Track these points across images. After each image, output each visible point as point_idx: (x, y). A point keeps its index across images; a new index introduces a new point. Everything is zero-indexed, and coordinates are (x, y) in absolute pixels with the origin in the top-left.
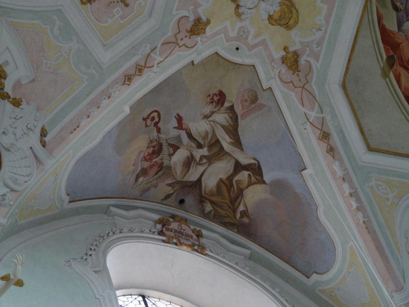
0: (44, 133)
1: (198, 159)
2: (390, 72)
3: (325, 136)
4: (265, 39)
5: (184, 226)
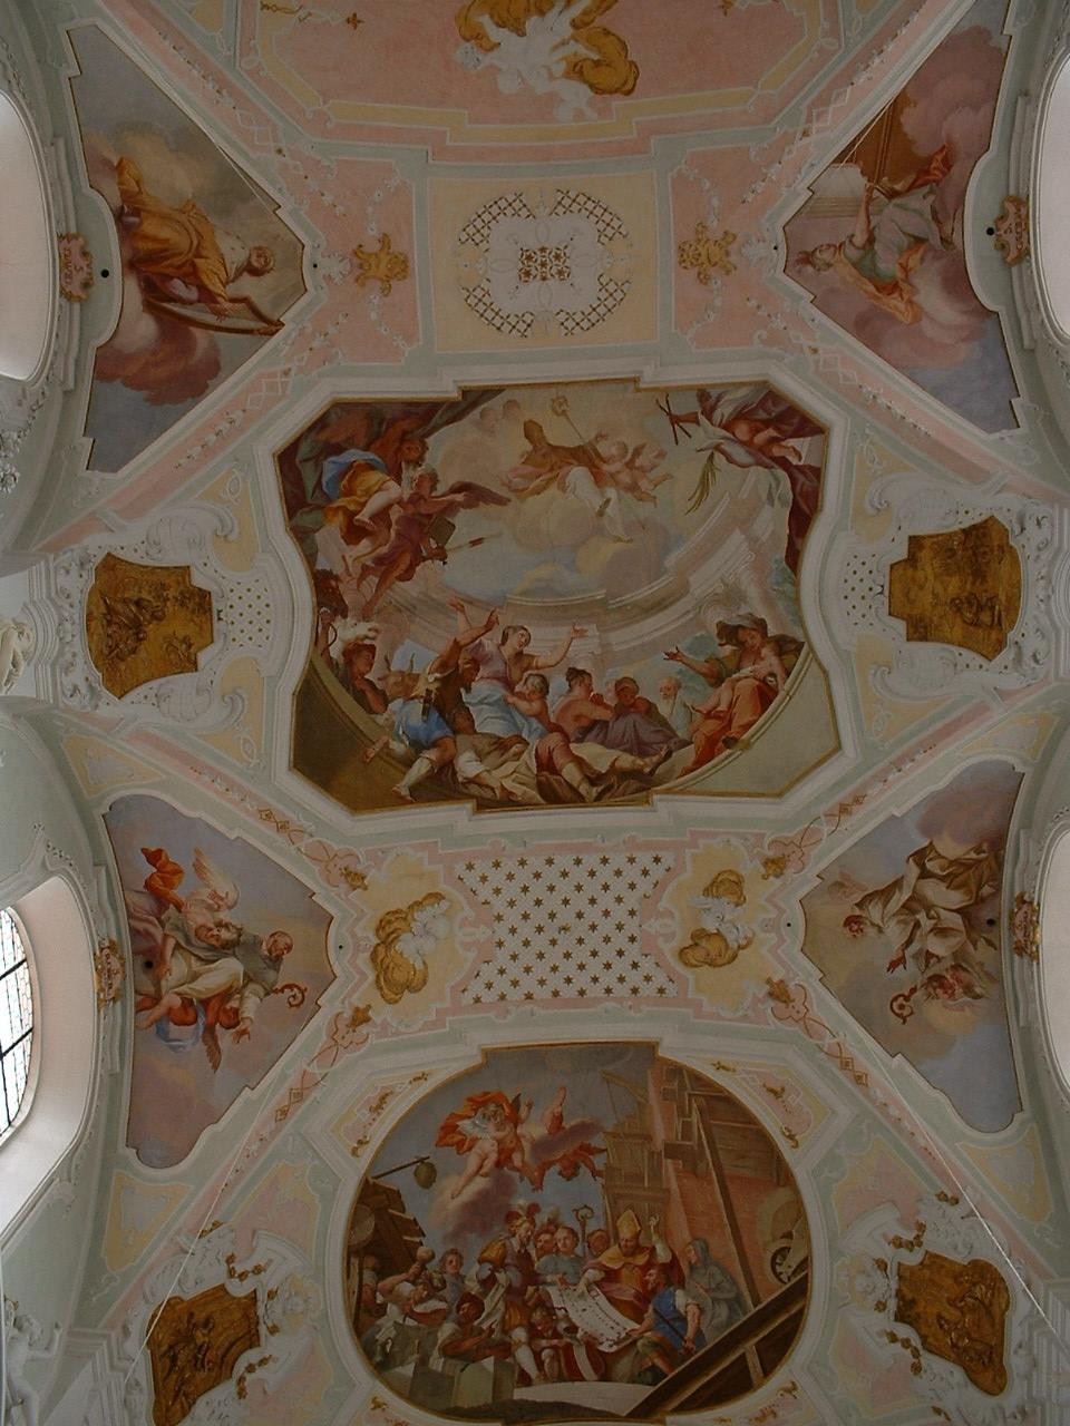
0: (942, 1197)
1: (933, 922)
2: (743, 741)
3: (844, 809)
4: (766, 900)
5: (1017, 922)
